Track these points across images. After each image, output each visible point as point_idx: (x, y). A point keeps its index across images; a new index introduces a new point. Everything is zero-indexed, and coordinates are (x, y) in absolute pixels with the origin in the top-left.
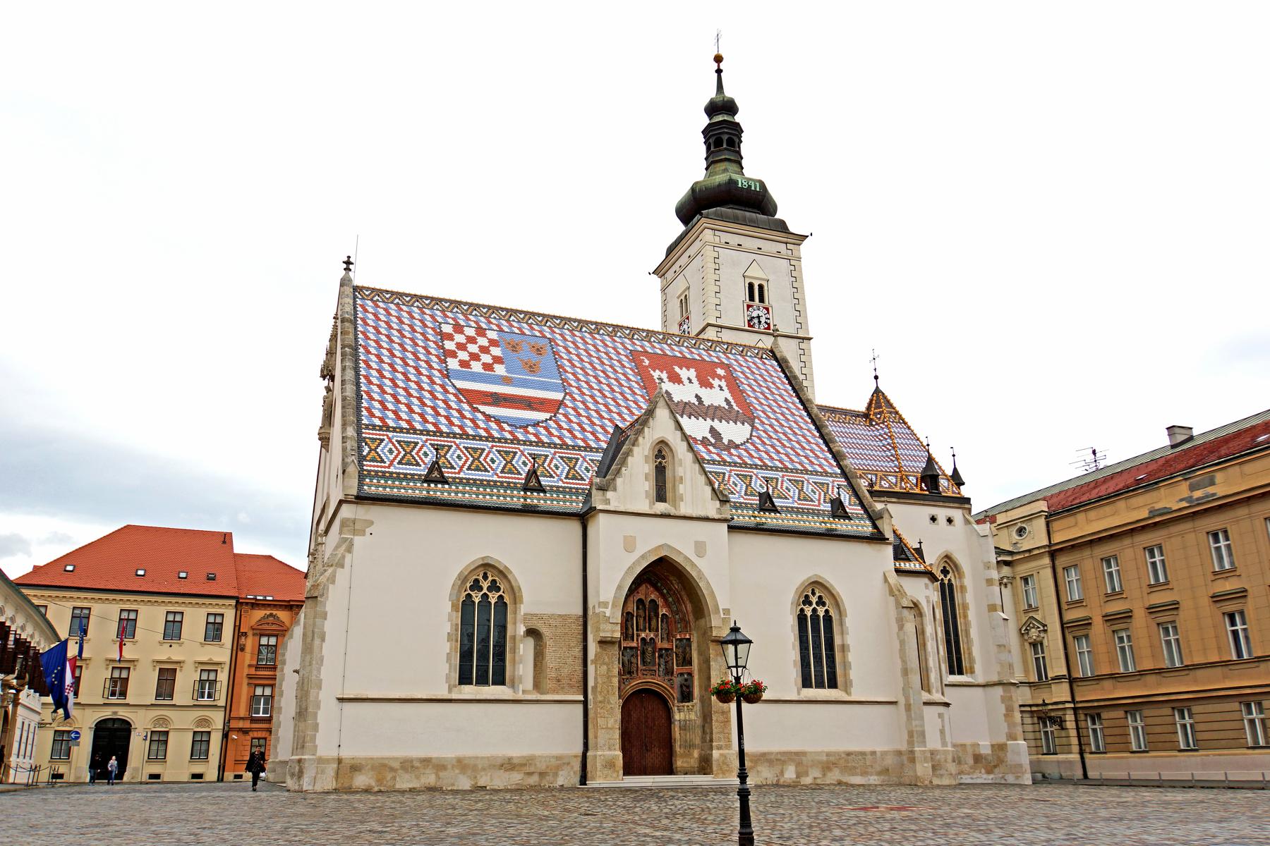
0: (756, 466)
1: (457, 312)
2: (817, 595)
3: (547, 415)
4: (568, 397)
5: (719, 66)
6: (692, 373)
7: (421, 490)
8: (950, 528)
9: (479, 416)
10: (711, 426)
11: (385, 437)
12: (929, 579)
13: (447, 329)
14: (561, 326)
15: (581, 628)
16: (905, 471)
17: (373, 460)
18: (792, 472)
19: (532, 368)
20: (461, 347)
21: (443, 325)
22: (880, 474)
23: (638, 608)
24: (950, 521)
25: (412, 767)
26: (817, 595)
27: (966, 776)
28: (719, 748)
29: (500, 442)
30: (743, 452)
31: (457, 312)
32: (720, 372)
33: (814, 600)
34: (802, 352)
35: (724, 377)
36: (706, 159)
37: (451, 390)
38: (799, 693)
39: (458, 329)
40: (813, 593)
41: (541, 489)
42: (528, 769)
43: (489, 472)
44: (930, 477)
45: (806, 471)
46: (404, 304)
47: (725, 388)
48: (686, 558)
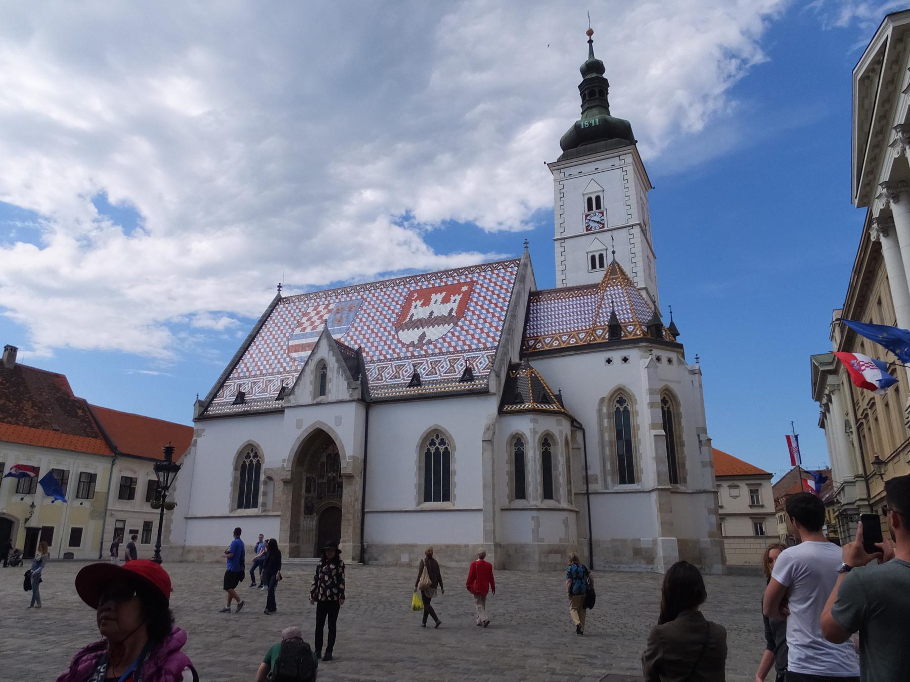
2: (440, 438)
5: (590, 38)
7: (238, 408)
9: (288, 360)
10: (424, 332)
16: (597, 326)
22: (573, 334)
24: (625, 360)
27: (625, 566)
28: (344, 542)
32: (465, 288)
33: (437, 442)
34: (632, 236)
35: (465, 293)
37: (285, 347)
38: (419, 504)
40: (437, 437)
44: (615, 328)
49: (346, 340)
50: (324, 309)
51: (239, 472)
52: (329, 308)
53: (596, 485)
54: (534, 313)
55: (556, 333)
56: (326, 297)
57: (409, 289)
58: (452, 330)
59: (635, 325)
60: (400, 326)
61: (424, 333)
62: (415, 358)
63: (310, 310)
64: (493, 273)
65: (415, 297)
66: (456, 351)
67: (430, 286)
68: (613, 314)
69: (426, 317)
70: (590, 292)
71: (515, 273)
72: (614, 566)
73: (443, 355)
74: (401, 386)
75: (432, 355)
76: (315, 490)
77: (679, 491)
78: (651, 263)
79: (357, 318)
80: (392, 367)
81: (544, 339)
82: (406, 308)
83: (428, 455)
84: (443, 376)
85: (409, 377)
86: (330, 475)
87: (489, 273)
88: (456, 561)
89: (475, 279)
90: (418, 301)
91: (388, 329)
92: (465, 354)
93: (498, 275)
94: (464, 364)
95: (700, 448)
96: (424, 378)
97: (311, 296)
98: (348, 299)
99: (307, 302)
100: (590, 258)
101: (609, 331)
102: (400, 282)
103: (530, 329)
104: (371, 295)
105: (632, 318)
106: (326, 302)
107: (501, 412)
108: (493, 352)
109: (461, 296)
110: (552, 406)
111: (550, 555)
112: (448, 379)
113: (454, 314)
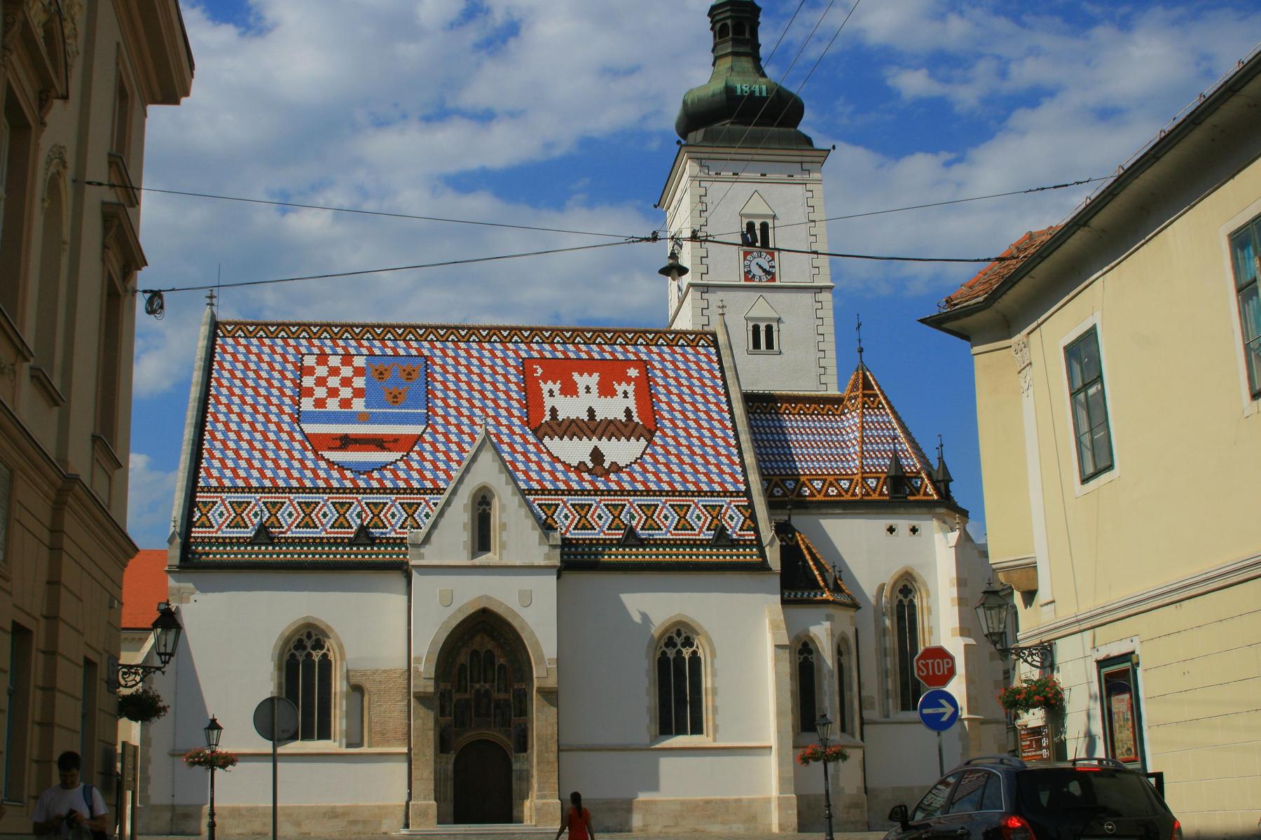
0: (635, 493)
1: (326, 338)
2: (684, 635)
3: (398, 455)
4: (429, 430)
6: (593, 380)
8: (915, 538)
9: (323, 464)
10: (596, 447)
11: (219, 500)
13: (309, 361)
14: (444, 338)
15: (406, 682)
17: (203, 526)
18: (680, 496)
19: (395, 399)
20: (321, 382)
21: (306, 358)
22: (830, 479)
23: (472, 661)
24: (914, 530)
25: (240, 815)
26: (684, 635)
29: (338, 493)
30: (625, 477)
31: (326, 338)
32: (633, 372)
33: (679, 641)
34: (819, 305)
36: (713, 51)
37: (298, 436)
39: (322, 358)
41: (372, 541)
42: (352, 818)
43: (318, 528)
45: (700, 493)
46: (267, 337)
47: (631, 394)
48: (508, 608)
51: (284, 673)
57: (516, 352)
61: (596, 449)
66: (674, 492)
81: (783, 481)
86: (477, 686)
88: (722, 823)
89: (644, 357)
96: (643, 534)
100: (750, 328)
101: (884, 483)
108: (743, 501)
113: (636, 419)
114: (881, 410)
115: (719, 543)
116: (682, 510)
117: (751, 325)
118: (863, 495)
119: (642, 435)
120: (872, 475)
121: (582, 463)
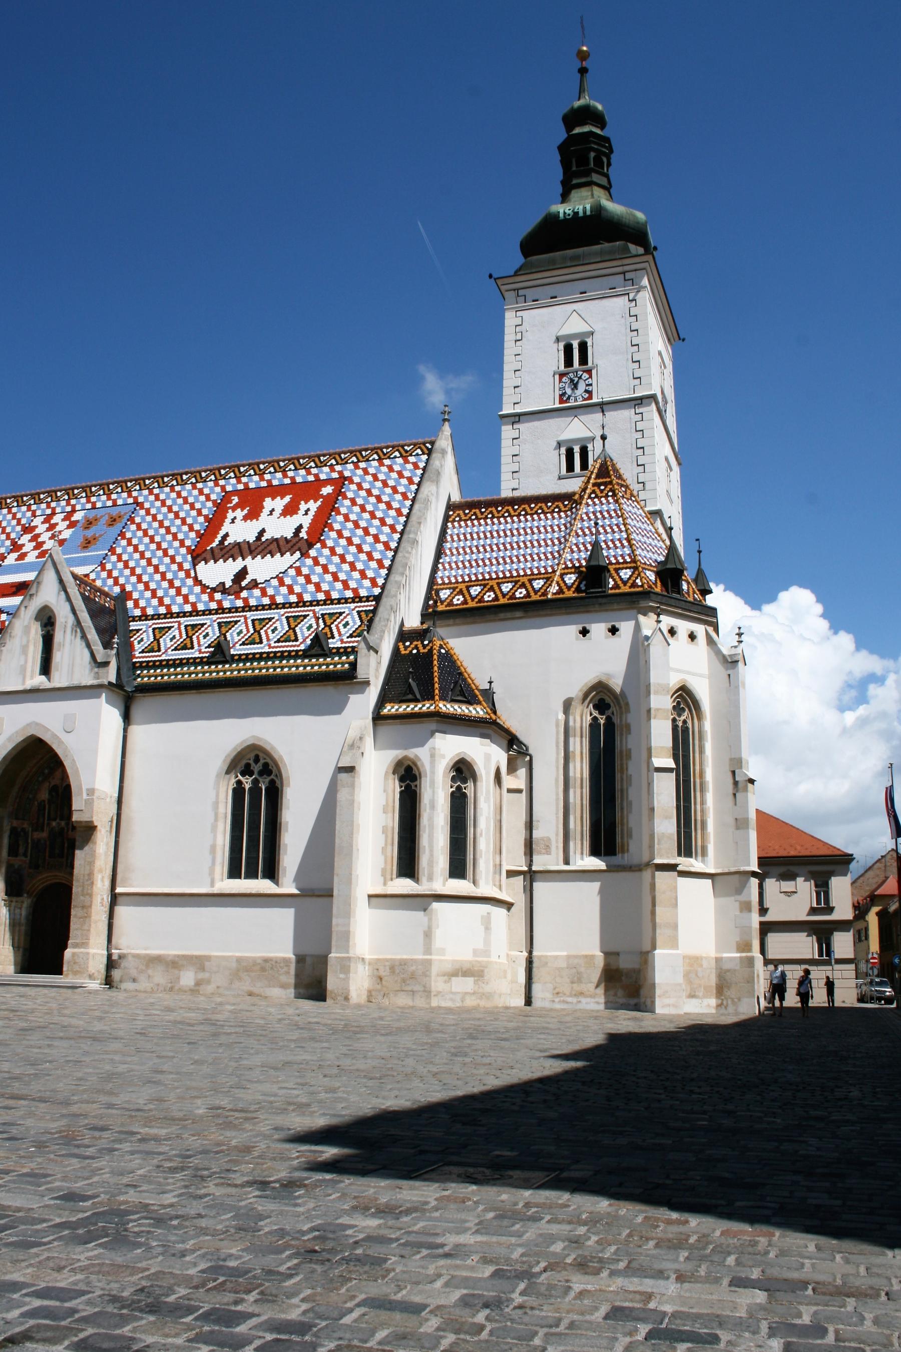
2: (262, 761)
10: (245, 566)
12: (438, 722)
24: (613, 630)
26: (262, 761)
27: (588, 1000)
28: (76, 946)
33: (256, 768)
40: (257, 759)
48: (55, 736)
49: (98, 577)
50: (63, 520)
52: (73, 519)
53: (546, 856)
54: (453, 541)
55: (491, 579)
56: (69, 499)
57: (223, 488)
58: (298, 564)
59: (635, 568)
60: (198, 555)
62: (223, 613)
63: (37, 521)
64: (382, 464)
65: (234, 502)
66: (301, 603)
67: (264, 484)
68: (596, 545)
69: (251, 539)
70: (557, 507)
71: (422, 465)
72: (570, 999)
73: (277, 608)
74: (195, 662)
75: (257, 608)
76: (26, 851)
77: (693, 869)
78: (671, 470)
79: (124, 537)
80: (179, 628)
82: (215, 522)
83: (238, 792)
84: (273, 647)
85: (209, 646)
86: (54, 824)
87: (375, 464)
89: (347, 474)
90: (239, 510)
91: (179, 559)
92: (317, 609)
93: (391, 468)
94: (315, 626)
95: (735, 795)
97: (42, 496)
98: (110, 503)
99: (34, 507)
102: (207, 476)
103: (445, 569)
104: (152, 498)
105: (629, 555)
106: (69, 509)
107: (378, 718)
108: (370, 606)
109: (319, 503)
110: (475, 709)
111: (453, 978)
112: (282, 652)
113: (303, 534)
114: (610, 498)
115: (313, 652)
116: (293, 622)
117: (563, 450)
118: (554, 594)
119: (299, 549)
120: (570, 571)
121: (223, 584)
